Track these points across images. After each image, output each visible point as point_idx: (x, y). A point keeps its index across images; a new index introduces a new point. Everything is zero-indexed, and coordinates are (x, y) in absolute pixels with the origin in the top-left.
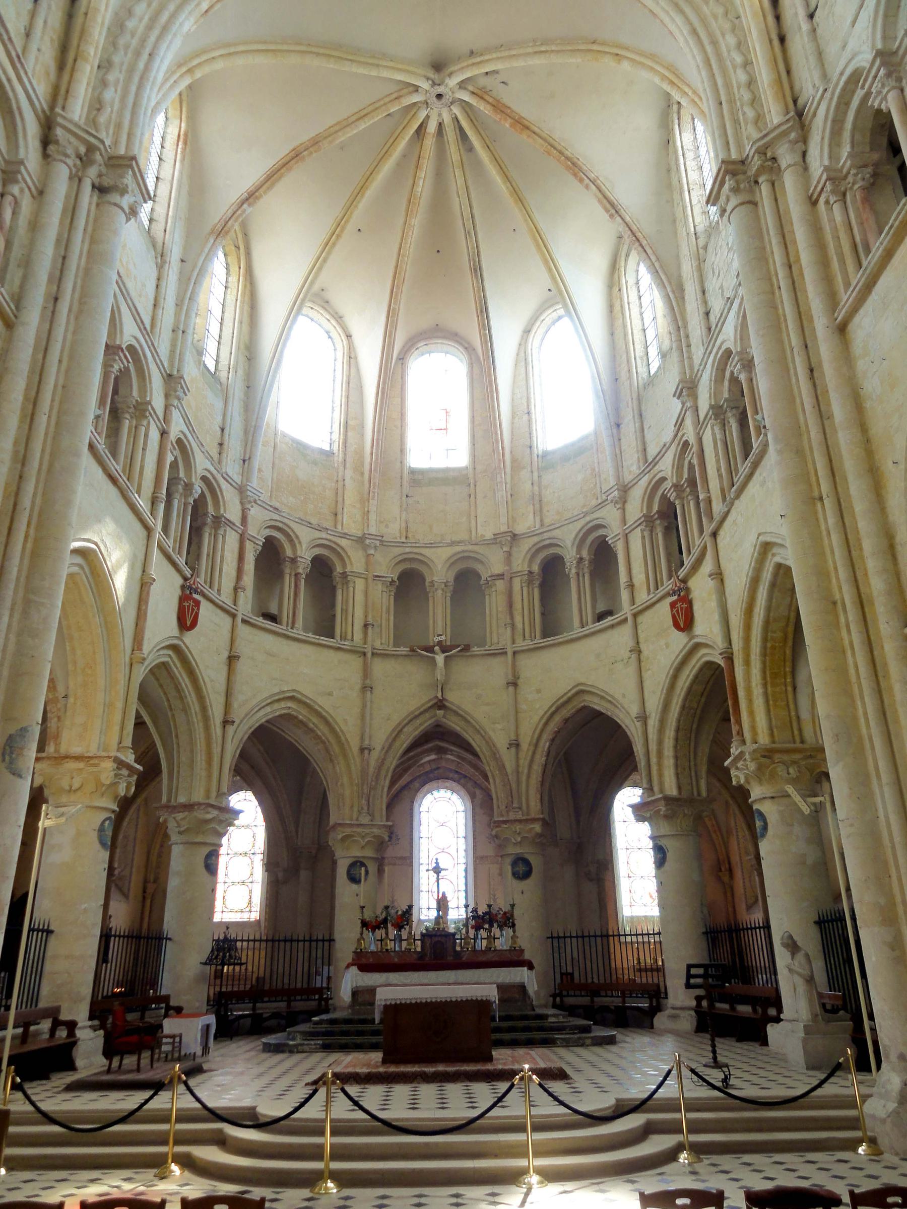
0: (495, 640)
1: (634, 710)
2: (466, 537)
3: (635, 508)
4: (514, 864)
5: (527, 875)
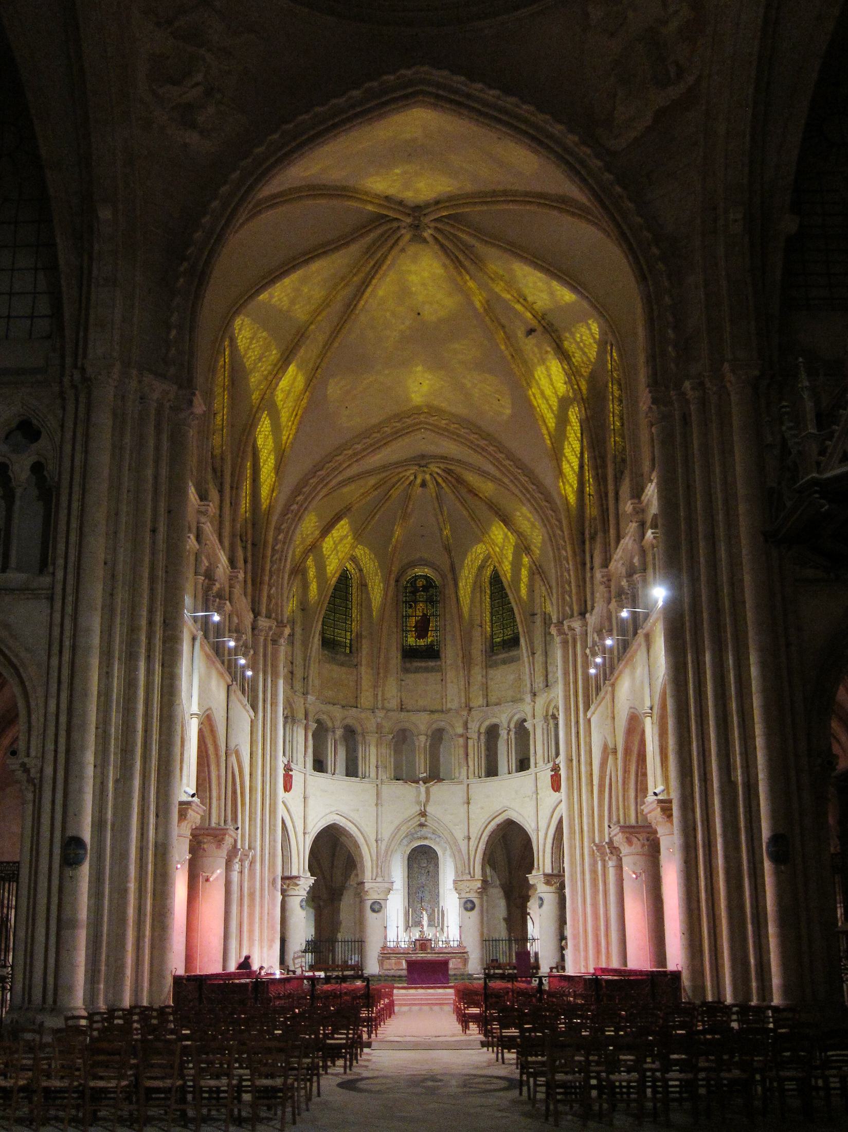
0: (457, 775)
1: (533, 825)
2: (440, 708)
3: (540, 712)
4: (466, 903)
5: (472, 909)
